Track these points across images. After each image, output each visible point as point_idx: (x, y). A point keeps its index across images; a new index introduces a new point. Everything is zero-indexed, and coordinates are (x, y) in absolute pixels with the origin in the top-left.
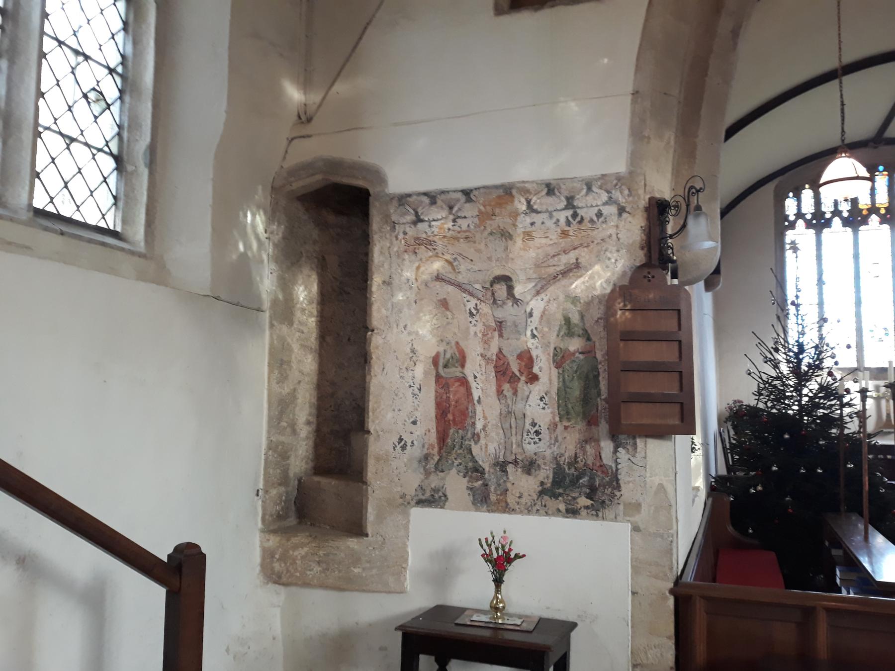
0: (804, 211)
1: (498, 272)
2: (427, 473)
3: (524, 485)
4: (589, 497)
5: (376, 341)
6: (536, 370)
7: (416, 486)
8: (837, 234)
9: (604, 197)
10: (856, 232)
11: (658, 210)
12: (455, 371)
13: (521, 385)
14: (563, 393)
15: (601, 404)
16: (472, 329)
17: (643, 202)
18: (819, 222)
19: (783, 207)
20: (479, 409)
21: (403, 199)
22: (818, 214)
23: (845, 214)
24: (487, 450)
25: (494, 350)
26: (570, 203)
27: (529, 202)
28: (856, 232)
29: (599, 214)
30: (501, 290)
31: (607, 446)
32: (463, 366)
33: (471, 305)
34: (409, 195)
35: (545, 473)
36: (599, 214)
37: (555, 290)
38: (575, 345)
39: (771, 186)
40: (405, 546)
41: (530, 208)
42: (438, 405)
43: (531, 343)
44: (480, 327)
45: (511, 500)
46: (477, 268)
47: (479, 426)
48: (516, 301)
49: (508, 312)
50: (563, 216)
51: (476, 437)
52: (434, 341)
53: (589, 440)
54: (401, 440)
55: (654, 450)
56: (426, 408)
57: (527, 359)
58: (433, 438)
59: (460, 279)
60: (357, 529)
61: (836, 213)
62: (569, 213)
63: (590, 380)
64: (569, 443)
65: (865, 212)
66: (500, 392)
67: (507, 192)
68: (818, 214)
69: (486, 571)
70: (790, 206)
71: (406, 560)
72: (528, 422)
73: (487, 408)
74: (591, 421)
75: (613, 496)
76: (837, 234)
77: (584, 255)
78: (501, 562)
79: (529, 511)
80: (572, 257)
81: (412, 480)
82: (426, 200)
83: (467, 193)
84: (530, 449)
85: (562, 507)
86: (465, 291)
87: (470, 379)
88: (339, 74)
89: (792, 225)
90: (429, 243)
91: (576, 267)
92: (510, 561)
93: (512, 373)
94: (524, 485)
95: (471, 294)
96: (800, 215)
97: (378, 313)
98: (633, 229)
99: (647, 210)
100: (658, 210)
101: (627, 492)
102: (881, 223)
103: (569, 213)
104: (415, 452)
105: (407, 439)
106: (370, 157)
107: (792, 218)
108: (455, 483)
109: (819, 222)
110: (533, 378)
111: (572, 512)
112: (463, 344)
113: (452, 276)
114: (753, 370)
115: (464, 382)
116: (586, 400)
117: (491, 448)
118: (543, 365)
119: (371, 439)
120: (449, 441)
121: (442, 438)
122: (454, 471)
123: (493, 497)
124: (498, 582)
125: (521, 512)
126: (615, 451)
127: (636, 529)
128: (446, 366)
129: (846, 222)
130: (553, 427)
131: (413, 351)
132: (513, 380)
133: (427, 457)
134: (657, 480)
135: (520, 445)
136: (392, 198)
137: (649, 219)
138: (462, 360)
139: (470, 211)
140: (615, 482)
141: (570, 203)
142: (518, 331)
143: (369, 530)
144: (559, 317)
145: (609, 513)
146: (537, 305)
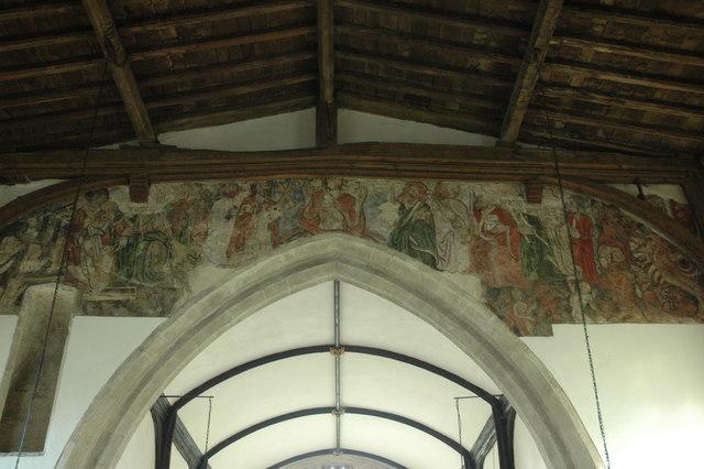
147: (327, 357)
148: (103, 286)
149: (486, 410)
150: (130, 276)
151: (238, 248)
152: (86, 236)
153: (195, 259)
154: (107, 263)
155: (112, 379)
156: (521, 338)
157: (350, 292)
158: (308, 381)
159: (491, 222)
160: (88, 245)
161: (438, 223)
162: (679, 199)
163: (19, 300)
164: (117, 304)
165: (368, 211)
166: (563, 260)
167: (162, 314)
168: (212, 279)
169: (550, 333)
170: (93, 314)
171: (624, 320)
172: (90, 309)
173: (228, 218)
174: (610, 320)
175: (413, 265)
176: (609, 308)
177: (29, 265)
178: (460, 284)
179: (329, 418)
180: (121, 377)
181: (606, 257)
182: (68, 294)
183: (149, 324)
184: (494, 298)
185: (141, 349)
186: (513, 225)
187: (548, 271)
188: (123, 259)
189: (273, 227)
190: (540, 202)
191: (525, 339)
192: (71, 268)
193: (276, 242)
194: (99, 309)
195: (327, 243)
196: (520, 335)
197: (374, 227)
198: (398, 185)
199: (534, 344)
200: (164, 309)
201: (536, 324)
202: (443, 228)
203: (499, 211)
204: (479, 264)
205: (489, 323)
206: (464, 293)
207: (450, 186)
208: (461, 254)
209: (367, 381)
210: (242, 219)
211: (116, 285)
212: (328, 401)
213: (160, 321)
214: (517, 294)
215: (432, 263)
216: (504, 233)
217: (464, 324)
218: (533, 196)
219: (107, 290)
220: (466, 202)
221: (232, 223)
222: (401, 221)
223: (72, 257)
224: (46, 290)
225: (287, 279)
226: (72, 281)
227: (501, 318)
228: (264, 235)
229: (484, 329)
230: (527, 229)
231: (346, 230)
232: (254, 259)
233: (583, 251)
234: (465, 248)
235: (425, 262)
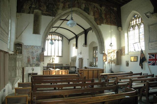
3: (34, 65)
14: (37, 59)
21: (25, 46)
24: (31, 63)
26: (37, 47)
35: (35, 64)
49: (33, 54)
53: (38, 62)
56: (27, 60)
57: (34, 57)
58: (27, 62)
61: (50, 39)
64: (37, 62)
74: (38, 61)
83: (30, 46)
98: (41, 49)
108: (29, 65)
111: (37, 67)
121: (28, 62)
141: (37, 47)
146: (35, 54)
148: (45, 11)
150: (49, 10)
151: (64, 8)
152: (42, 3)
153: (58, 9)
154: (45, 8)
155: (48, 25)
159: (96, 9)
160: (42, 4)
161: (90, 8)
162: (116, 10)
163: (33, 12)
164: (47, 14)
165: (81, 5)
166: (103, 16)
167: (54, 17)
168: (60, 11)
170: (44, 15)
171: (109, 25)
172: (44, 15)
173: (62, 3)
174: (107, 24)
175: (86, 14)
176: (107, 23)
177: (33, 6)
178: (91, 17)
180: (49, 25)
181: (108, 16)
182: (40, 12)
184: (95, 19)
186: (98, 10)
187: (102, 17)
188: (47, 7)
189: (69, 5)
190: (102, 7)
191: (98, 25)
192: (40, 7)
193: (69, 8)
194: (45, 15)
195: (76, 9)
197: (82, 7)
198: (85, 2)
201: (99, 24)
202: (90, 9)
203: (97, 8)
204: (94, 15)
205: (94, 23)
206: (92, 18)
207: (91, 3)
208: (92, 13)
210: (64, 4)
211: (47, 11)
214: (98, 19)
215: (88, 14)
216: (97, 11)
217: (91, 22)
218: (101, 6)
219: (46, 12)
220: (93, 6)
221: (63, 4)
222: (85, 7)
223: (40, 6)
224: (36, 11)
225: (70, 13)
226: (40, 10)
227: (96, 22)
228: (67, 6)
229: (94, 23)
230: (100, 11)
231: (78, 7)
232: (66, 10)
233: (106, 15)
234: (92, 12)
235: (88, 13)
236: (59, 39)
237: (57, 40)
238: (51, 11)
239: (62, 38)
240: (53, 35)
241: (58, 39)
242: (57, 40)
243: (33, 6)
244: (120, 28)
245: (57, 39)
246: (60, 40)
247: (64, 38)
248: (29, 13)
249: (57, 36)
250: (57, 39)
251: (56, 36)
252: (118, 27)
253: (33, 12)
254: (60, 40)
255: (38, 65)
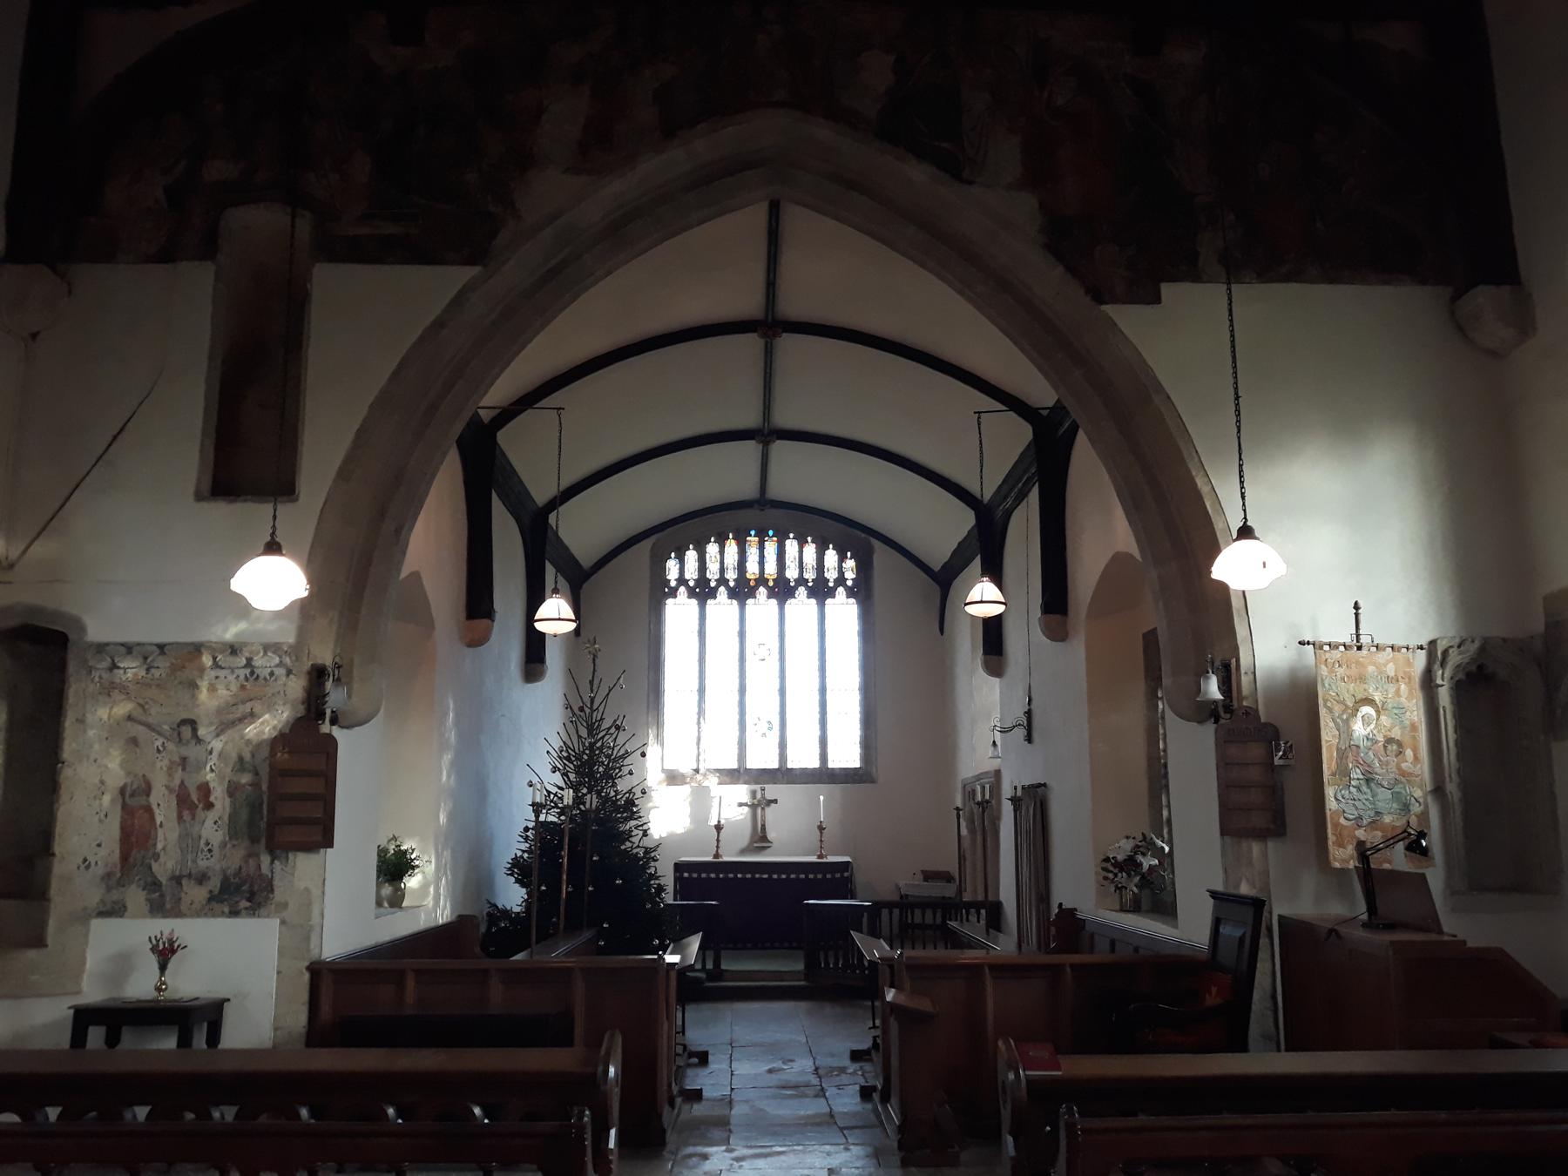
0: (687, 576)
1: (185, 716)
2: (109, 889)
3: (196, 894)
4: (249, 900)
5: (66, 774)
6: (212, 799)
7: (97, 899)
8: (722, 607)
9: (277, 660)
10: (742, 606)
11: (318, 674)
12: (142, 801)
13: (199, 811)
14: (233, 818)
15: (263, 825)
16: (159, 764)
17: (307, 665)
18: (702, 591)
19: (663, 570)
20: (160, 832)
21: (101, 648)
22: (702, 580)
23: (732, 584)
24: (164, 868)
25: (177, 782)
27: (214, 658)
28: (742, 606)
29: (272, 674)
30: (186, 731)
31: (265, 859)
32: (148, 795)
33: (158, 743)
34: (107, 644)
35: (215, 884)
36: (272, 674)
37: (230, 734)
38: (245, 779)
39: (647, 544)
40: (84, 952)
41: (216, 665)
42: (123, 829)
43: (210, 777)
44: (166, 762)
45: (183, 908)
46: (164, 713)
47: (160, 846)
48: (199, 741)
49: (193, 752)
50: (243, 673)
51: (156, 857)
52: (122, 773)
54: (85, 860)
55: (303, 862)
56: (112, 831)
57: (205, 790)
59: (150, 720)
60: (39, 942)
61: (722, 581)
62: (248, 671)
63: (254, 808)
64: (235, 859)
65: (752, 583)
66: (180, 817)
67: (197, 649)
68: (702, 580)
69: (153, 962)
70: (672, 568)
71: (84, 964)
72: (203, 842)
73: (167, 832)
74: (254, 840)
75: (267, 898)
76: (722, 607)
77: (258, 707)
78: (165, 953)
79: (198, 916)
80: (247, 708)
81: (94, 896)
82: (123, 650)
83: (161, 647)
84: (203, 864)
85: (226, 910)
86: (154, 730)
87: (154, 807)
88: (43, 529)
89: (673, 593)
90: (123, 689)
91: (252, 716)
92: (173, 952)
93: (191, 802)
94: (196, 894)
95: (159, 734)
96: (682, 581)
97: (68, 749)
98: (296, 687)
99: (309, 673)
100: (318, 674)
101: (279, 895)
102: (769, 597)
103: (248, 671)
104: (100, 871)
105: (92, 859)
106: (71, 608)
107: (673, 584)
108: (135, 896)
109: (702, 591)
110: (210, 806)
111: (234, 913)
112: (150, 776)
113: (143, 718)
114: (535, 780)
115: (149, 810)
116: (252, 823)
117: (170, 865)
118: (219, 795)
119: (56, 860)
120: (131, 860)
121: (125, 857)
122: (133, 887)
123: (168, 906)
124: (163, 968)
125: (192, 916)
126: (272, 862)
127: (283, 922)
128: (132, 795)
129: (733, 594)
130: (223, 845)
131: (102, 782)
132: (193, 808)
133: (109, 875)
134: (302, 885)
135: (194, 861)
136: (91, 645)
137: (310, 681)
138: (147, 790)
139: (163, 663)
140: (270, 888)
142: (200, 766)
143: (49, 941)
144: (234, 756)
145: (263, 911)
146: (217, 745)
147: (751, 343)
149: (1024, 433)
151: (600, 146)
155: (395, 375)
156: (1104, 307)
157: (799, 222)
158: (720, 385)
167: (470, 261)
169: (1157, 300)
175: (919, 174)
177: (219, 170)
178: (1000, 212)
179: (749, 450)
183: (449, 280)
184: (1062, 239)
185: (439, 324)
191: (1108, 309)
196: (1102, 302)
199: (1129, 319)
200: (476, 253)
205: (1050, 283)
209: (817, 385)
212: (749, 418)
213: (474, 271)
227: (1071, 270)
236: (831, 575)
237: (802, 591)
238: (437, 194)
239: (864, 568)
240: (762, 536)
241: (821, 579)
242: (802, 591)
243: (219, 170)
244: (1483, 297)
245: (801, 581)
246: (841, 580)
247: (881, 554)
248: (166, 256)
249: (802, 543)
250: (810, 575)
251: (791, 546)
252: (1455, 298)
253: (208, 249)
254: (841, 580)
255: (242, 894)
